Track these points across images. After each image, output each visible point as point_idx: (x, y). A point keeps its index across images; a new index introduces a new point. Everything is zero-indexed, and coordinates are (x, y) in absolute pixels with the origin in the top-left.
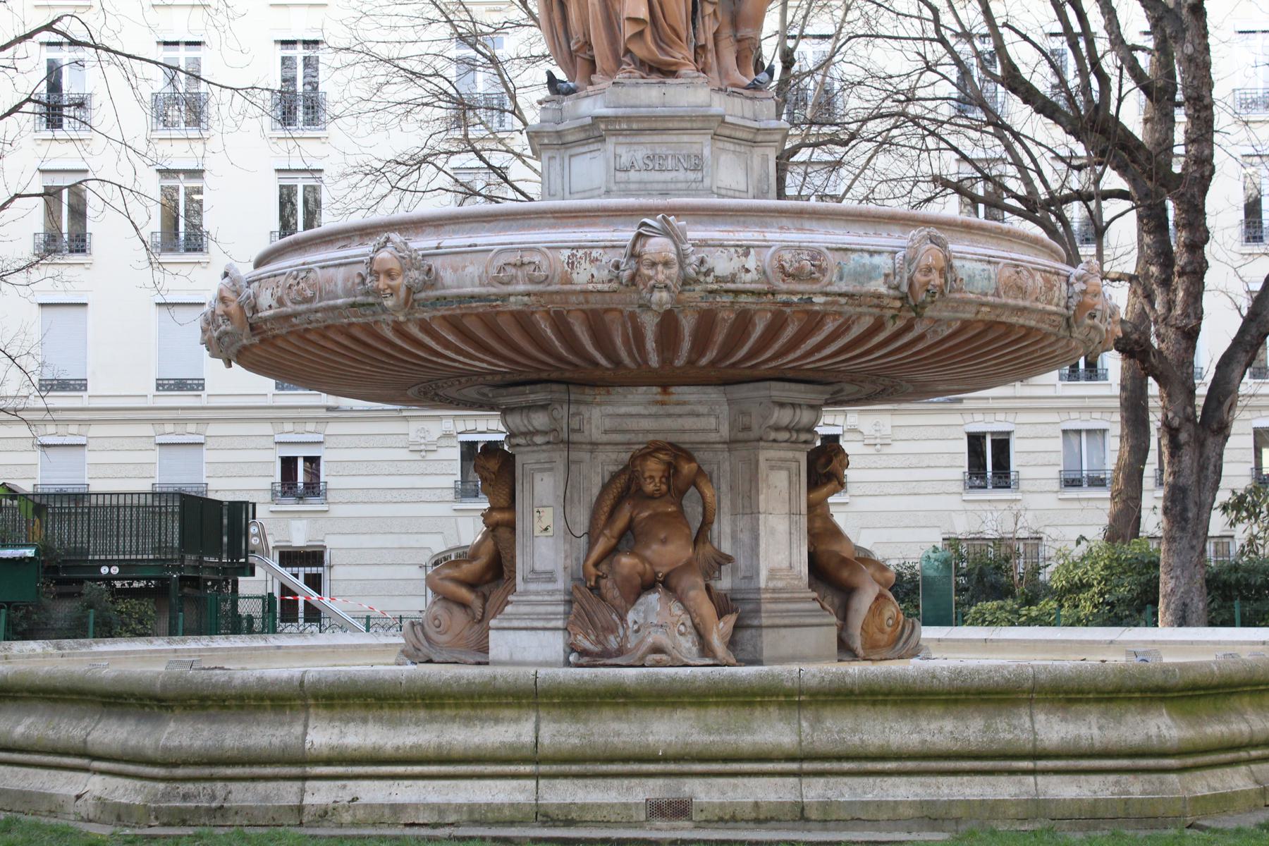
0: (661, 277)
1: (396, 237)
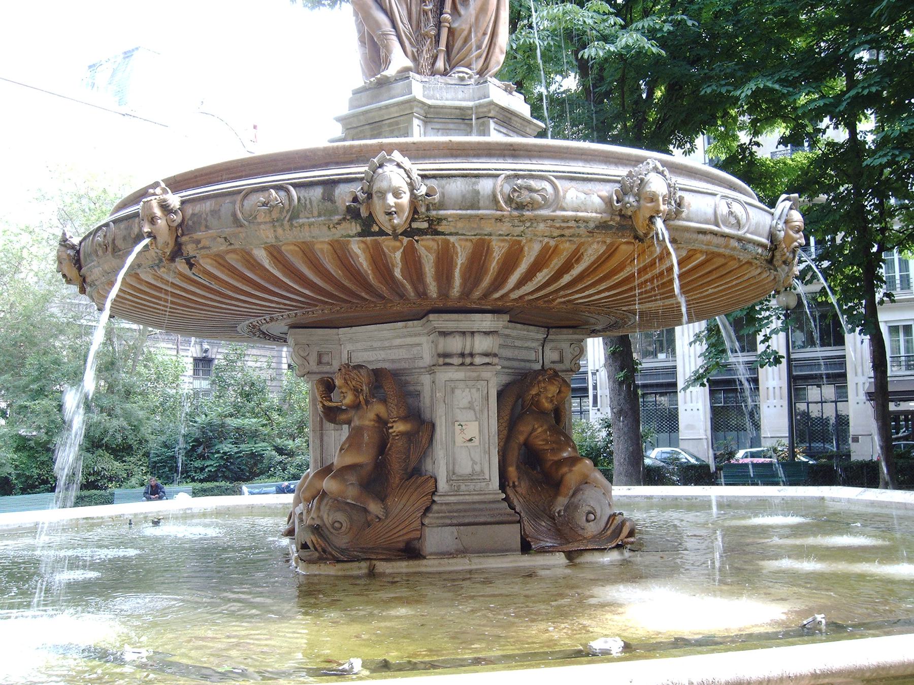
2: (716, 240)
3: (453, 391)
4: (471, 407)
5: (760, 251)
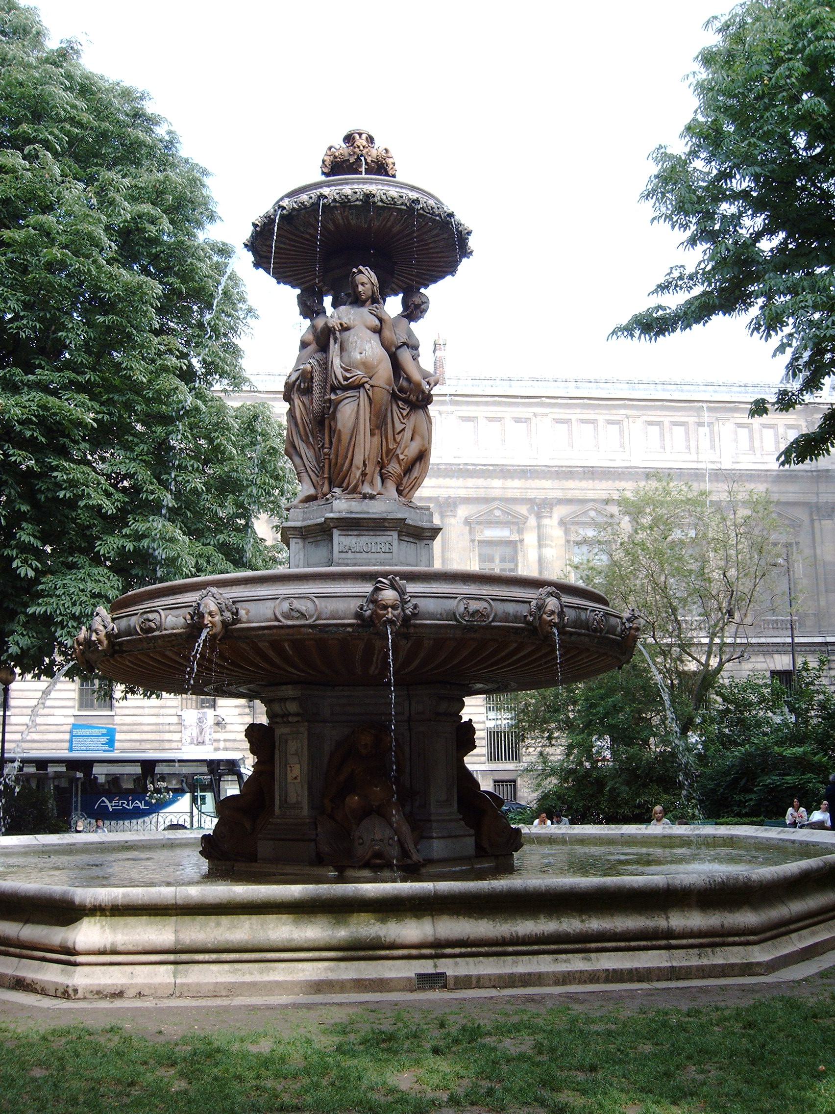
0: (390, 615)
1: (214, 590)
2: (283, 631)
3: (286, 741)
4: (296, 754)
5: (349, 629)
